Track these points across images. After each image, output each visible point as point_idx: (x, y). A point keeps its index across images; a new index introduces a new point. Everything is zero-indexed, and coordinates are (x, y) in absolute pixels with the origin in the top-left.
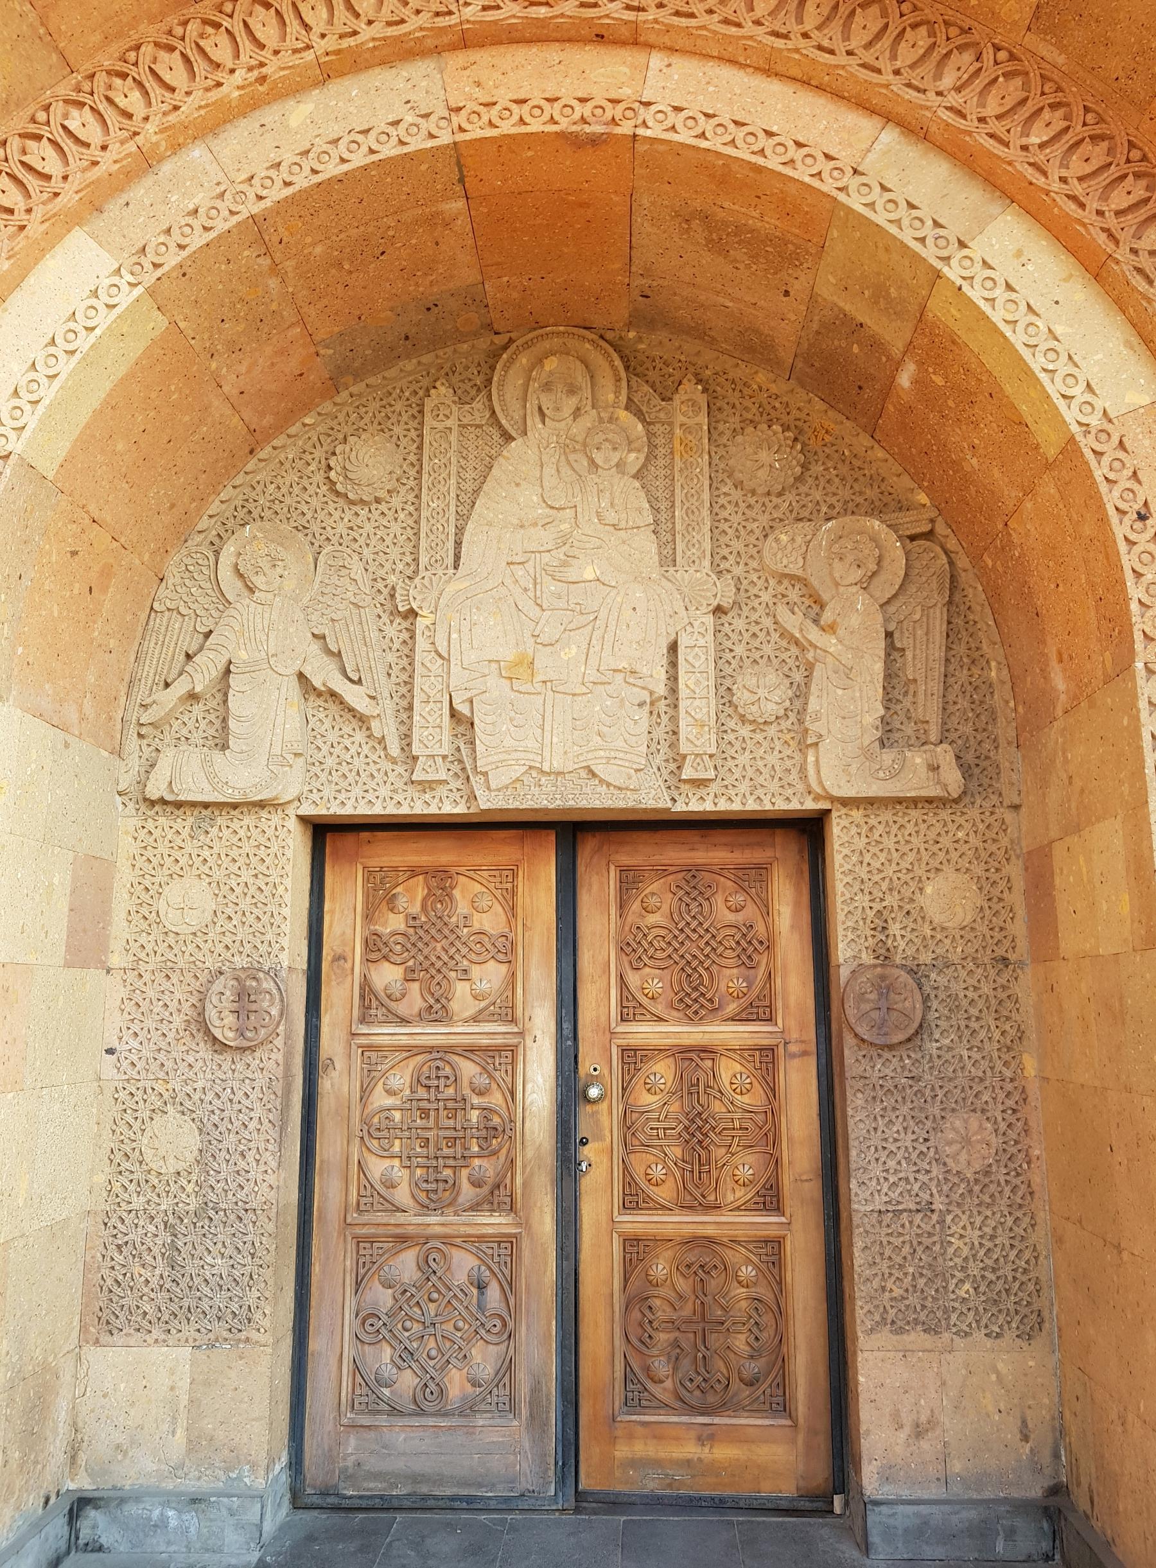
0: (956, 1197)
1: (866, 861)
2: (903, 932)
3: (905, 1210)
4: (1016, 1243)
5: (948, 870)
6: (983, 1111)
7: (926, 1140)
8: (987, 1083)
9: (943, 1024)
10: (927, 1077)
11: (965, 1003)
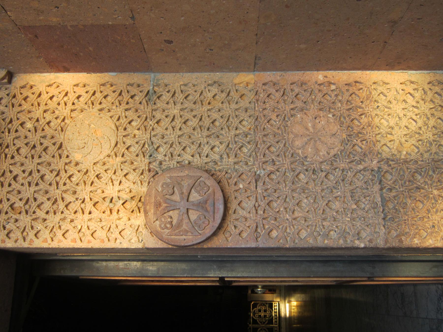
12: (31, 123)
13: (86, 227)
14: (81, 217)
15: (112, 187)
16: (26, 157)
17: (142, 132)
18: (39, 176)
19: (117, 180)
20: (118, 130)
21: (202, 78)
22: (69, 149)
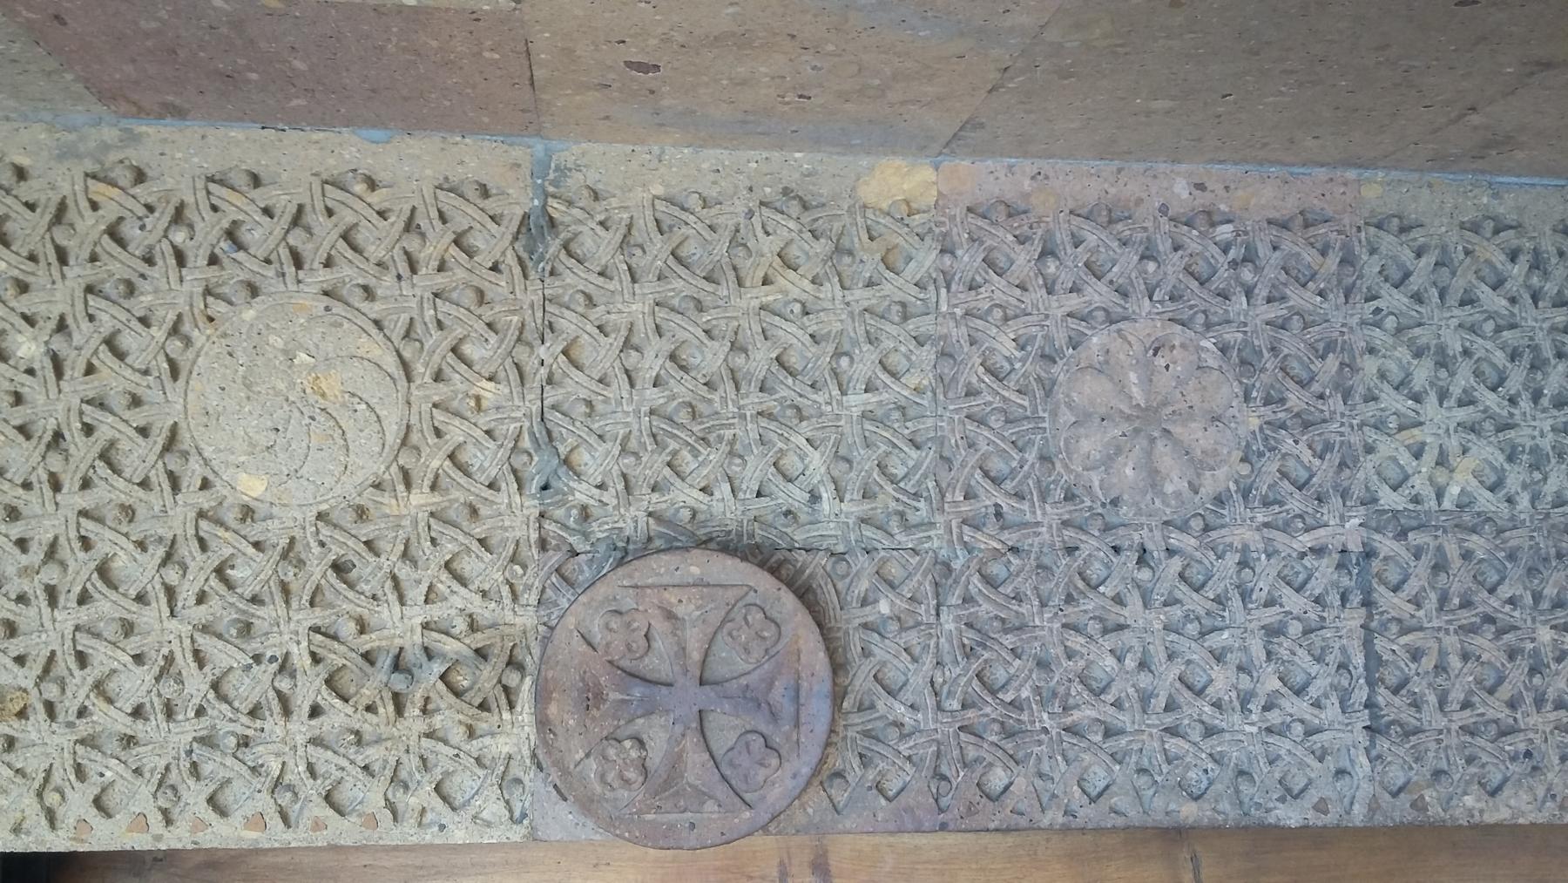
0: (1324, 472)
1: (124, 724)
2: (416, 594)
3: (1367, 644)
4: (1458, 285)
5: (167, 405)
6: (1048, 358)
7: (1143, 558)
8: (959, 333)
9: (754, 471)
10: (937, 541)
11: (683, 388)
12: (35, 339)
13: (302, 768)
14: (279, 731)
15: (397, 608)
16: (27, 486)
17: (507, 391)
18: (93, 565)
19: (419, 582)
20: (409, 379)
21: (739, 171)
22: (208, 452)
